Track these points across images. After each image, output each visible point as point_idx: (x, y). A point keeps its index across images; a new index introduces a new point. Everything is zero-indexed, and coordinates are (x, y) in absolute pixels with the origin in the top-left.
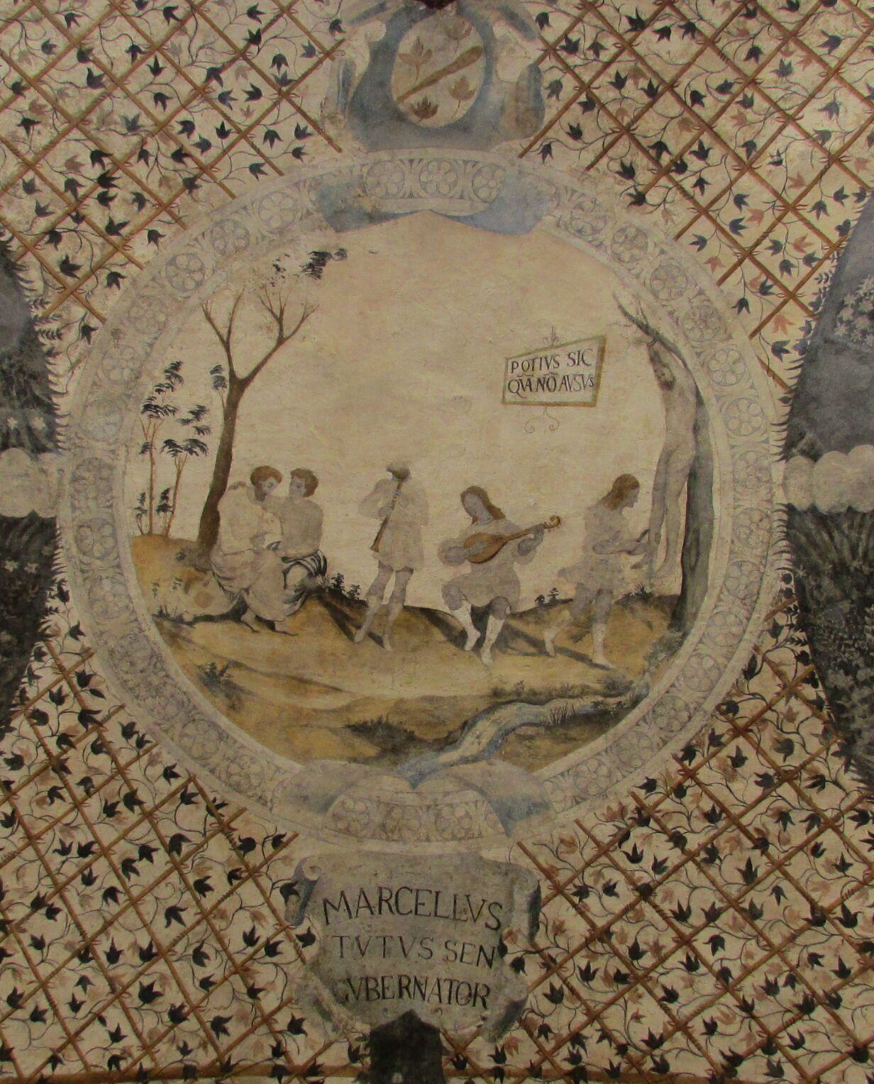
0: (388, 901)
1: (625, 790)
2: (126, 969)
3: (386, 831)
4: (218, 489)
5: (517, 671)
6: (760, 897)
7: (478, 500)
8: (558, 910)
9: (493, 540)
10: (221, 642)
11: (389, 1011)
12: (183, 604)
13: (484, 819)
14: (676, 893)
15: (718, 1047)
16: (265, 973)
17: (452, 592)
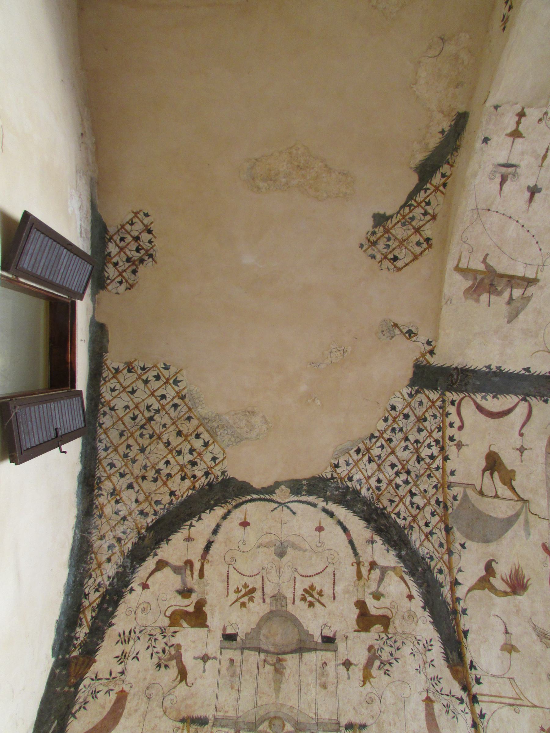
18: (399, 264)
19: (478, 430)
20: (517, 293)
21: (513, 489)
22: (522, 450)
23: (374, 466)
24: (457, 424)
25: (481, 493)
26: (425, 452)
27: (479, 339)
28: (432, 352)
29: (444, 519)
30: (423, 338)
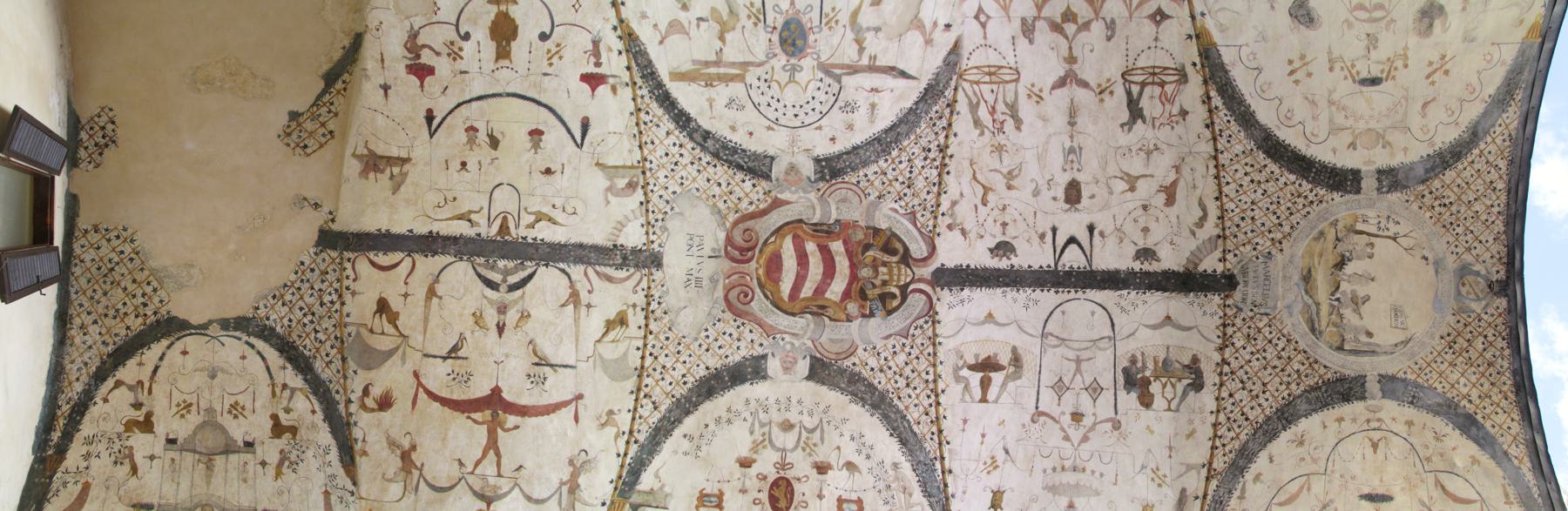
0: (1267, 278)
1: (1295, 336)
2: (1249, 213)
3: (1284, 277)
4: (1369, 234)
5: (1325, 309)
6: (1269, 370)
7: (1367, 299)
8: (1265, 320)
9: (1357, 302)
10: (1331, 236)
11: (1240, 278)
12: (1340, 226)
13: (1287, 302)
14: (1270, 349)
15: (1232, 360)
16: (1249, 247)
17: (1344, 293)
18: (309, 151)
19: (369, 281)
20: (396, 170)
21: (396, 327)
22: (406, 295)
23: (286, 309)
24: (352, 276)
25: (371, 331)
26: (327, 299)
27: (372, 208)
28: (333, 220)
29: (341, 351)
30: (326, 209)
